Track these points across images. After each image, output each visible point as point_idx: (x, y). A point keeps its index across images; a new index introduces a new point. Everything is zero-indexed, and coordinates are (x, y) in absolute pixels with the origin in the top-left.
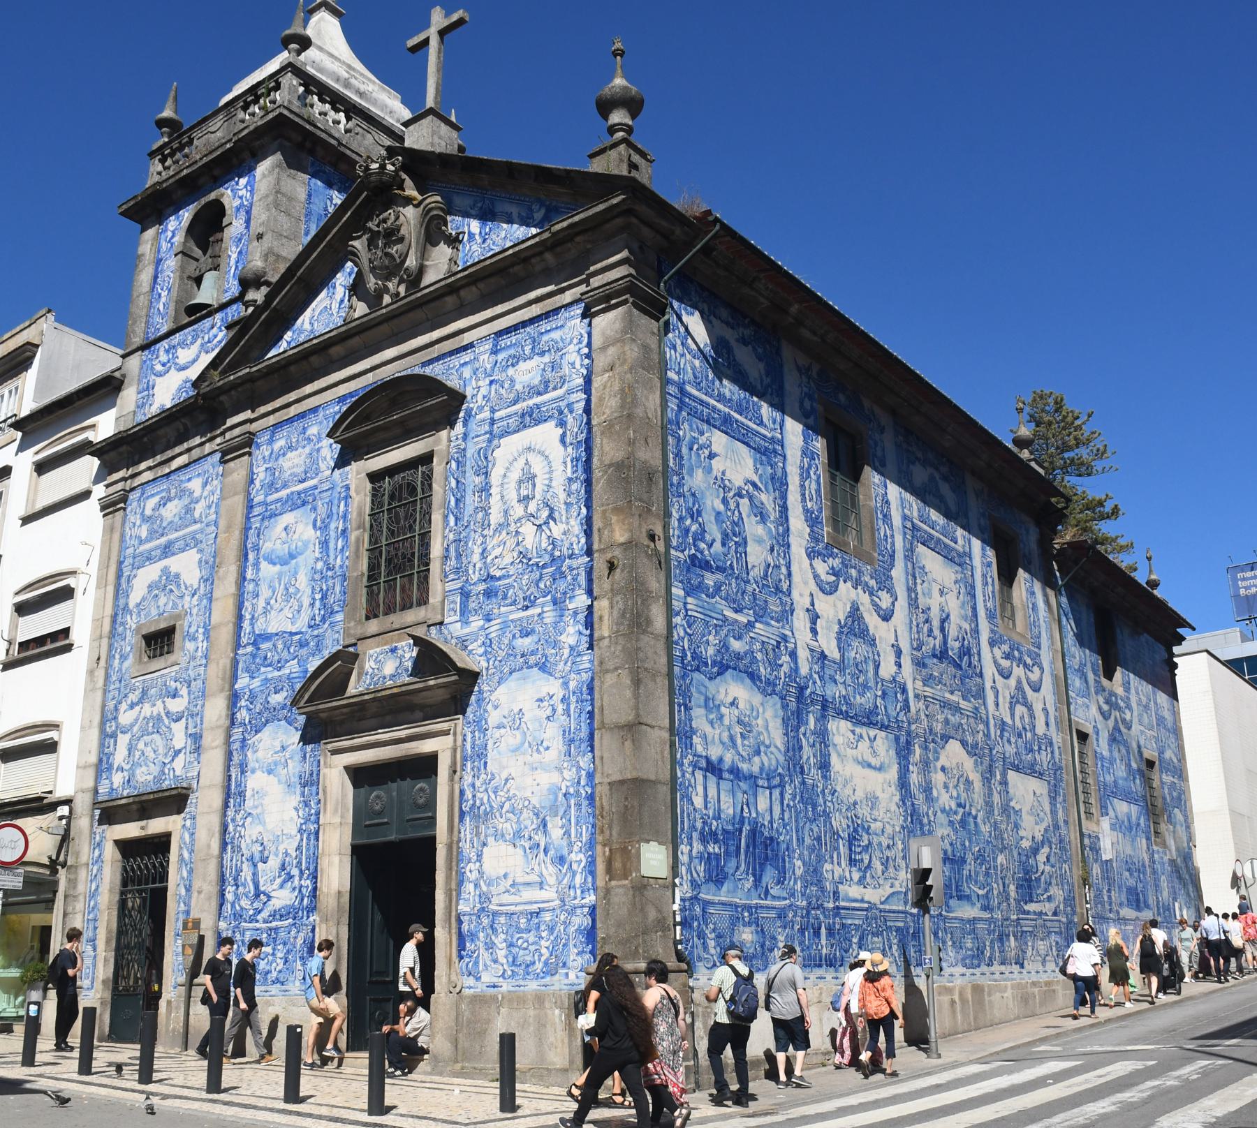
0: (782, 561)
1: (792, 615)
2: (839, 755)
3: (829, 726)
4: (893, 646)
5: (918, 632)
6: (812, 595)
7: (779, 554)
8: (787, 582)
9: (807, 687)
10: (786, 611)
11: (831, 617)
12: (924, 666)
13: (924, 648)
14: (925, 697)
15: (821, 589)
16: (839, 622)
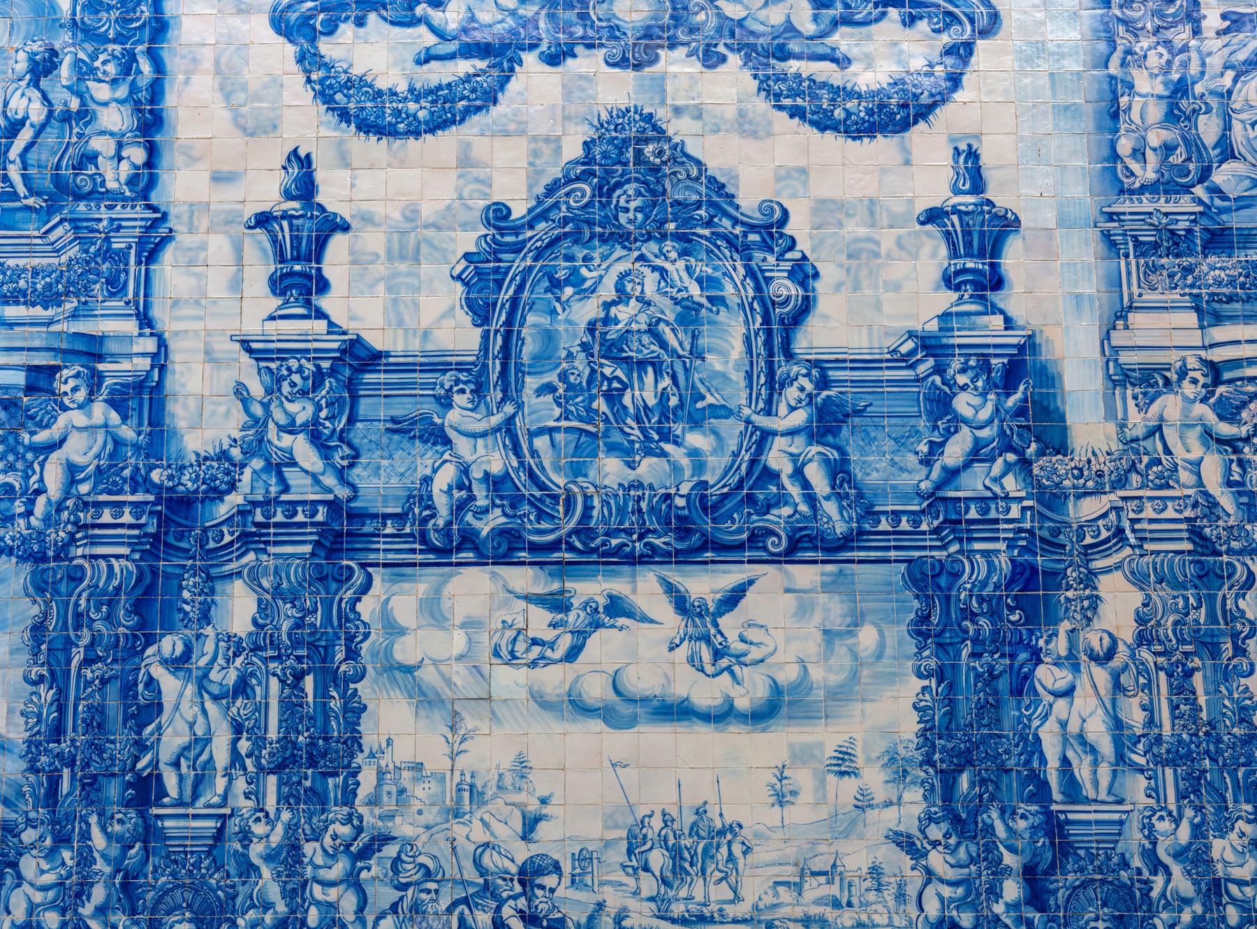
0: (101, 91)
1: (151, 251)
2: (425, 699)
3: (367, 608)
4: (933, 216)
5: (1173, 116)
6: (301, 162)
7: (84, 72)
8: (137, 155)
9: (217, 494)
10: (123, 255)
11: (428, 211)
12: (1218, 240)
13: (1222, 176)
14: (1215, 371)
15: (367, 127)
16: (498, 215)
